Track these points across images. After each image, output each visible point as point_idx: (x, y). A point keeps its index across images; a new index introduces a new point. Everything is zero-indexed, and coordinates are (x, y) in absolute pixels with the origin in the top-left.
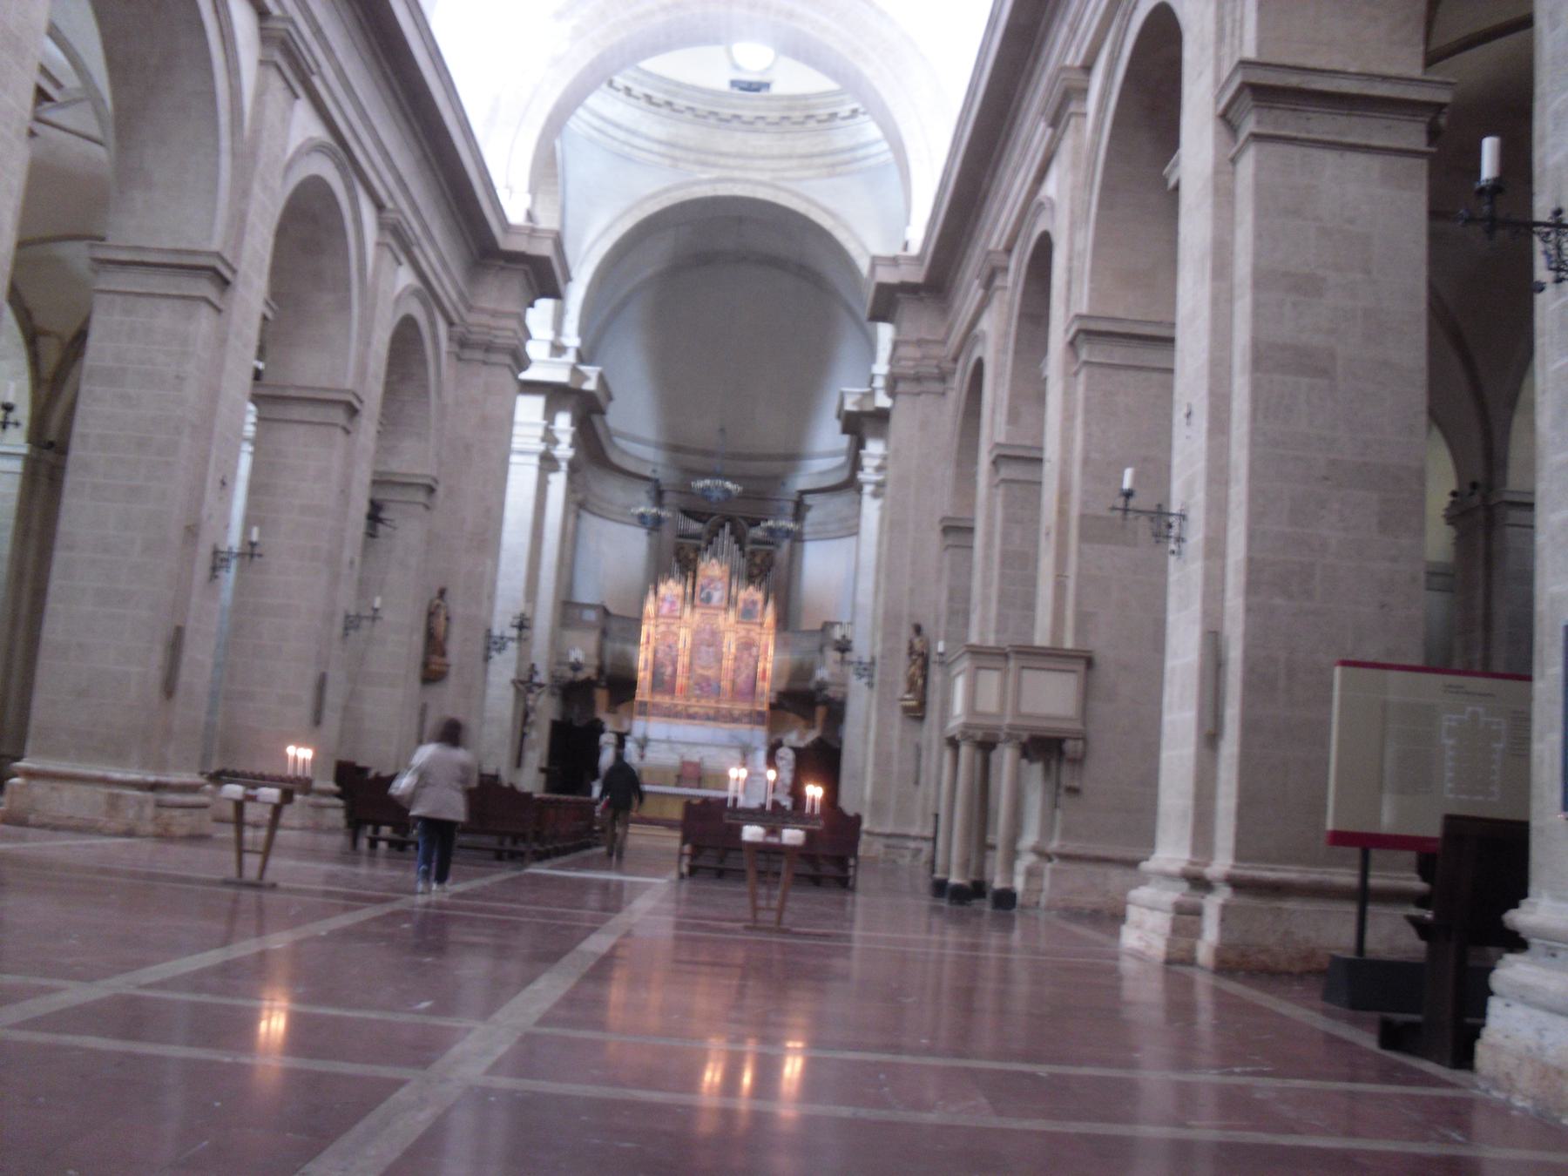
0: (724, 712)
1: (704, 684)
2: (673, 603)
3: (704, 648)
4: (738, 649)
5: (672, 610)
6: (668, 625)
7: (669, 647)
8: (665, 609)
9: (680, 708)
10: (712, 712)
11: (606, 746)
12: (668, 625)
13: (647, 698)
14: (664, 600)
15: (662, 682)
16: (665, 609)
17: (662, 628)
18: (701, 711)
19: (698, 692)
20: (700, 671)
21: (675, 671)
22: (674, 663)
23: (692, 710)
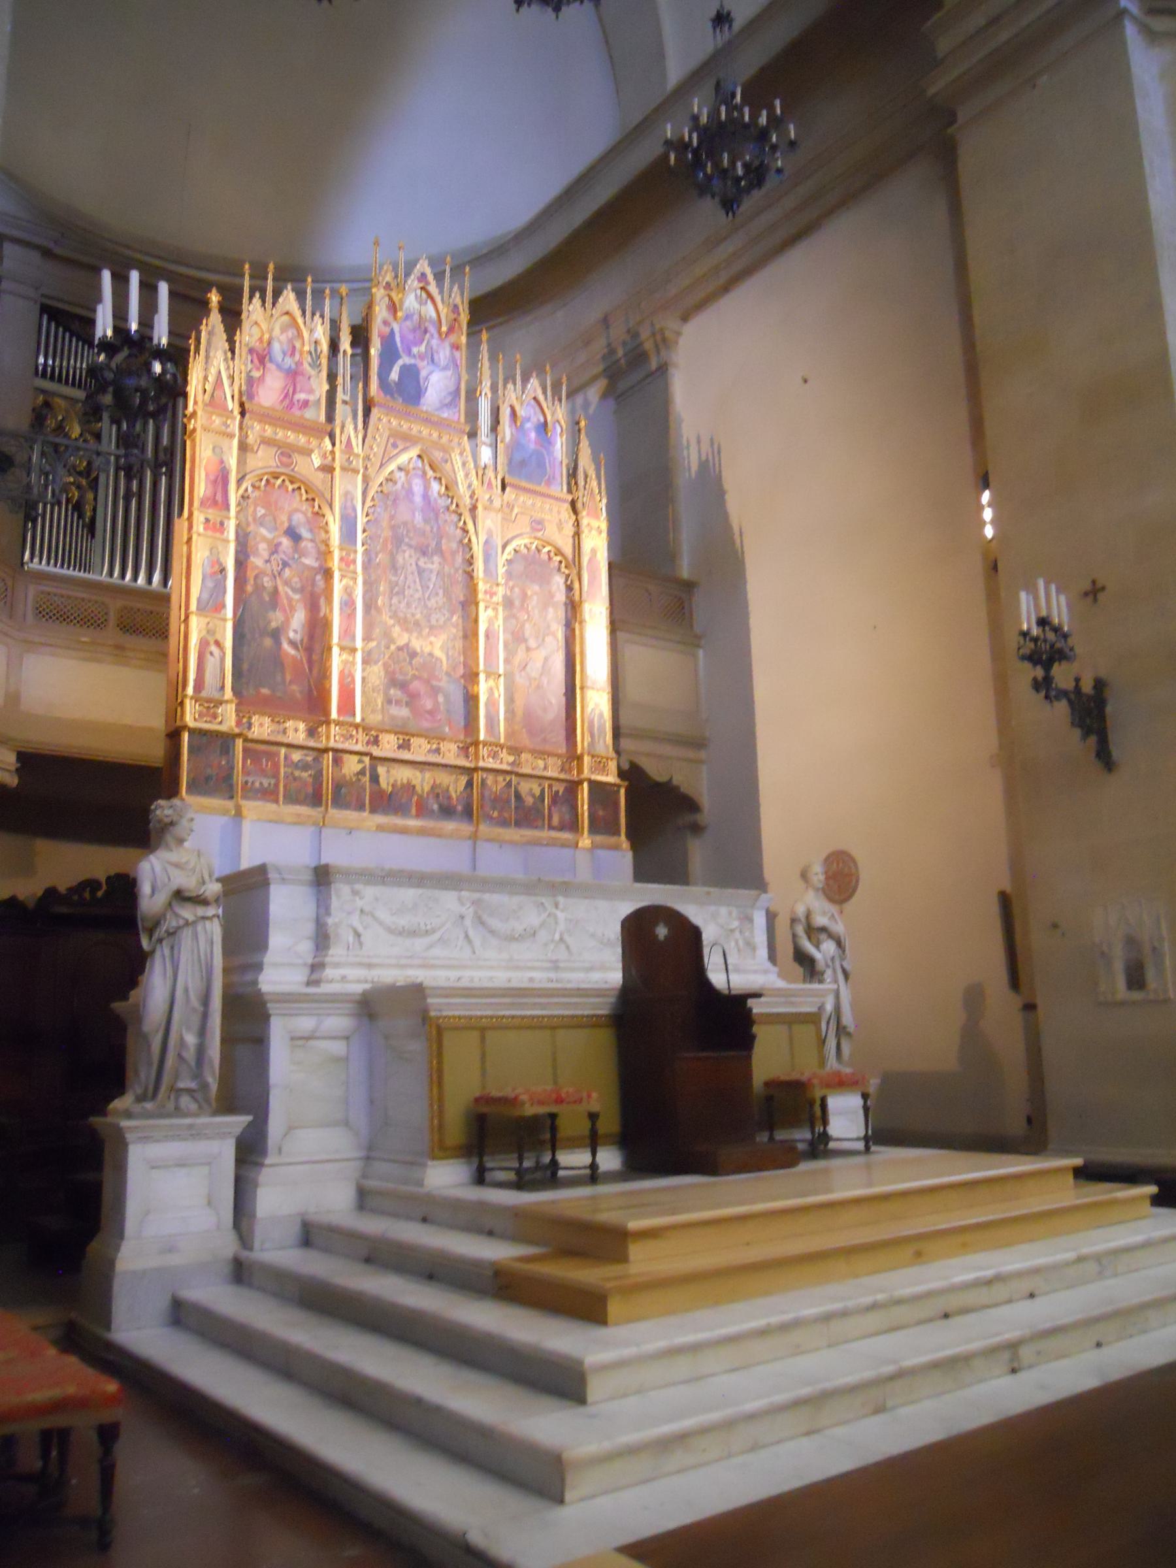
0: (496, 785)
1: (416, 685)
2: (293, 375)
3: (407, 557)
4: (509, 575)
5: (288, 396)
6: (286, 452)
7: (293, 534)
8: (269, 394)
9: (352, 765)
10: (455, 785)
11: (187, 912)
12: (286, 452)
13: (228, 719)
14: (262, 357)
15: (277, 659)
16: (269, 394)
17: (263, 460)
18: (423, 781)
19: (403, 712)
20: (401, 637)
21: (318, 628)
22: (315, 603)
23: (388, 777)
